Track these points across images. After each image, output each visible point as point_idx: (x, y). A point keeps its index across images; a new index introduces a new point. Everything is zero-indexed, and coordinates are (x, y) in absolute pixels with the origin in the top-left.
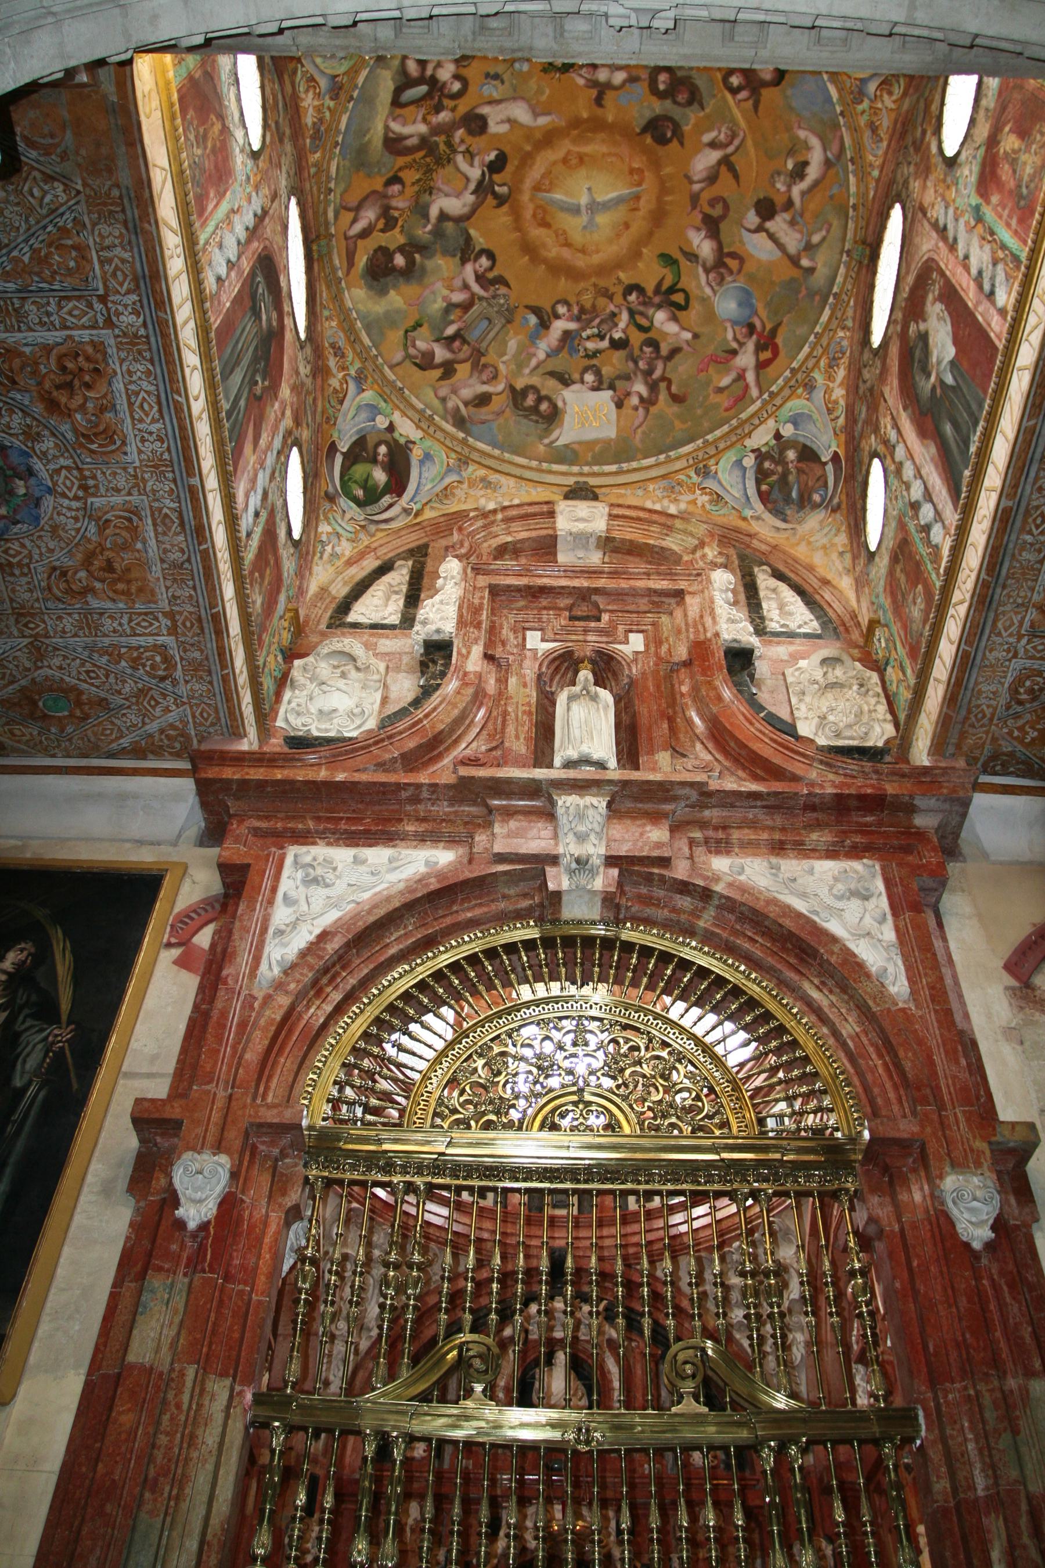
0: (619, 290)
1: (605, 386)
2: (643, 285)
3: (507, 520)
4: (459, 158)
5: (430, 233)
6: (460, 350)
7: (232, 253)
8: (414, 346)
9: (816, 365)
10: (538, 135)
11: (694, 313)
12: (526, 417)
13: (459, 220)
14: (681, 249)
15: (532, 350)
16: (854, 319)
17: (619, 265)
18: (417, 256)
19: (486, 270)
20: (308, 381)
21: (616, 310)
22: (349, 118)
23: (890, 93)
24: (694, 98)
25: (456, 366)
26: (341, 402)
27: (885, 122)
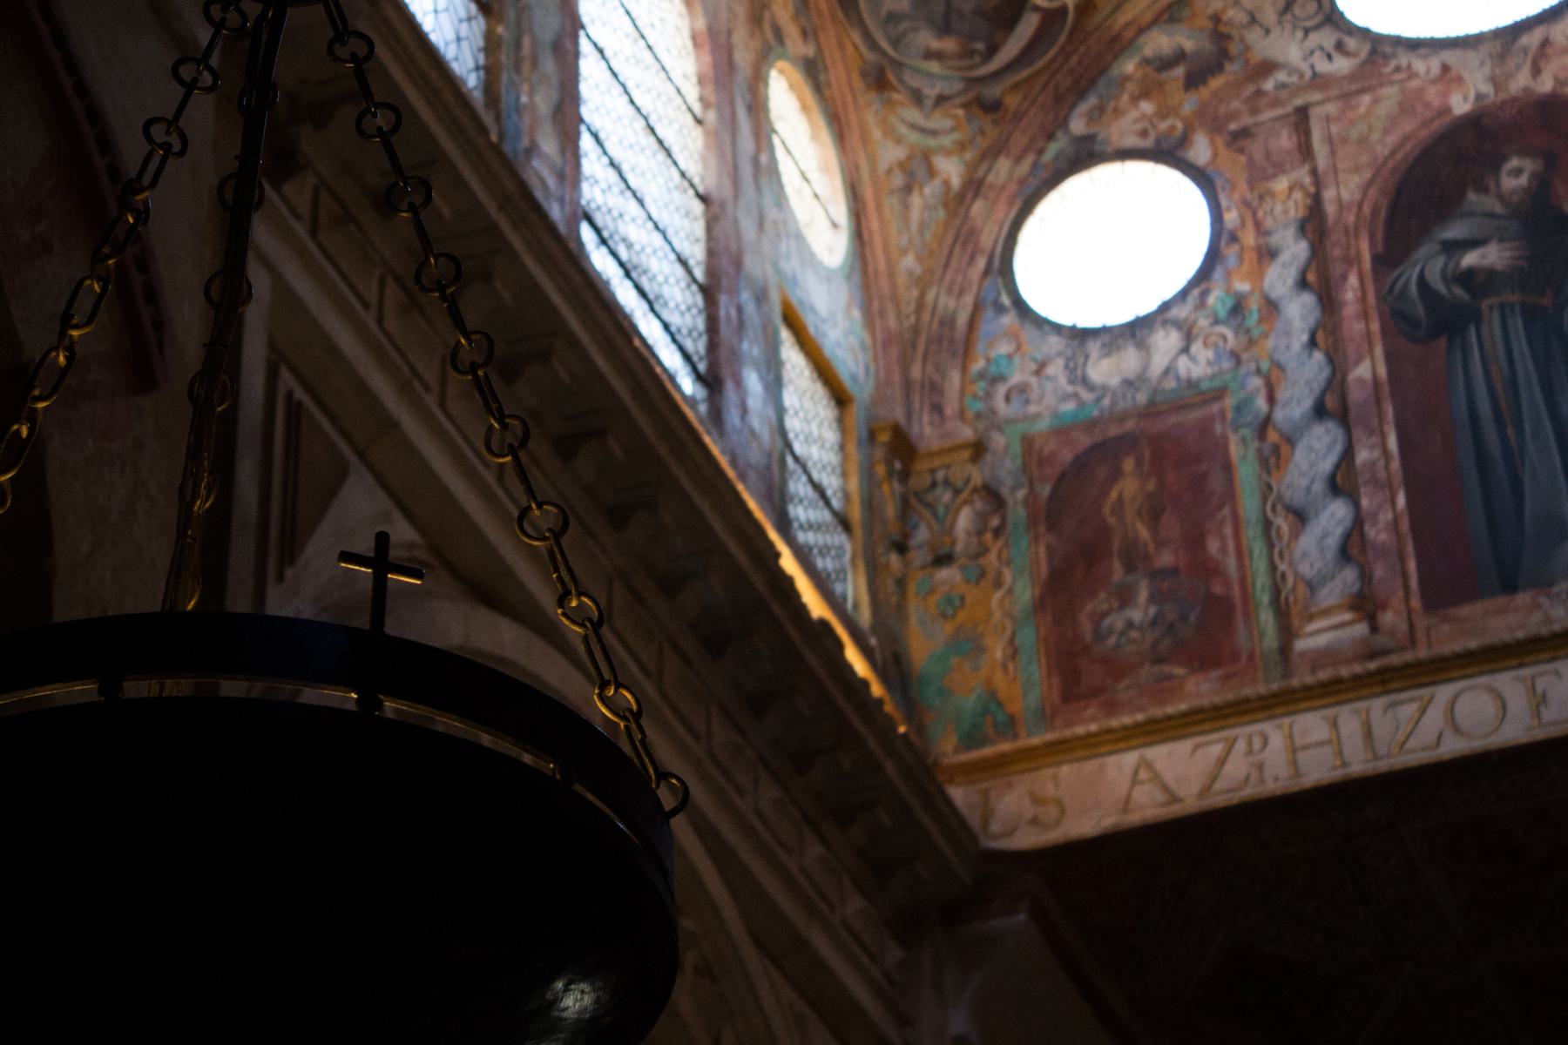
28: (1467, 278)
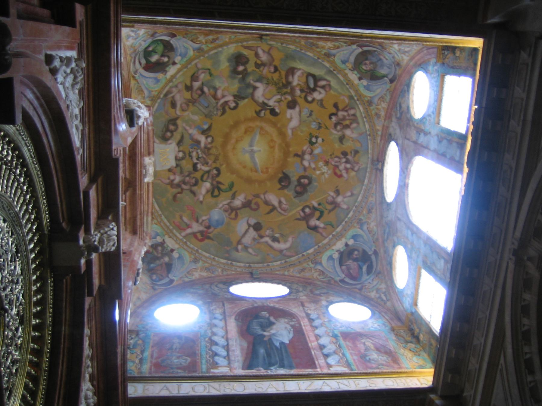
0: (218, 165)
1: (178, 162)
2: (220, 176)
4: (278, 97)
5: (250, 82)
6: (196, 93)
8: (202, 73)
9: (205, 262)
11: (210, 200)
13: (252, 95)
14: (236, 192)
16: (227, 275)
18: (241, 76)
19: (229, 106)
21: (209, 165)
23: (319, 275)
24: (299, 194)
26: (192, 41)
27: (307, 274)
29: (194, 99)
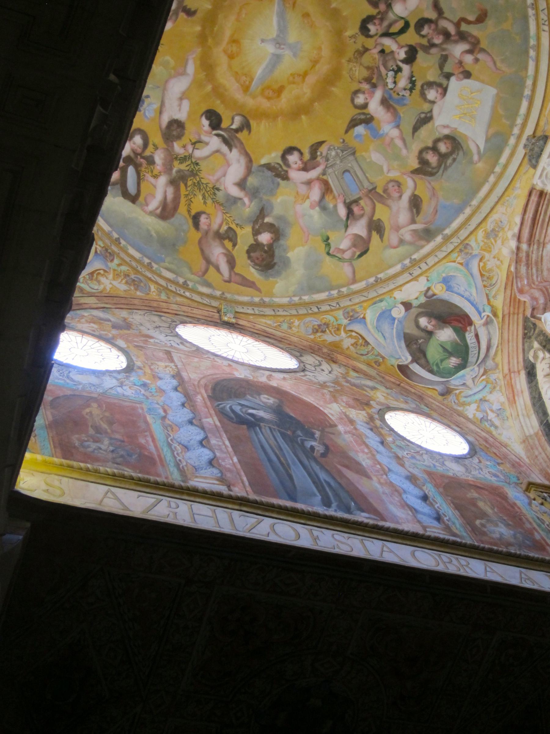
0: (361, 39)
1: (444, 82)
2: (364, 16)
3: (530, 242)
4: (198, 154)
5: (251, 201)
6: (363, 209)
7: (195, 434)
8: (344, 251)
10: (202, 75)
12: (446, 168)
13: (249, 171)
15: (387, 140)
17: (338, 33)
18: (267, 220)
19: (301, 160)
20: (338, 370)
21: (379, 48)
22: (133, 246)
25: (375, 218)
26: (367, 343)
28: (252, 415)
29: (370, 198)
